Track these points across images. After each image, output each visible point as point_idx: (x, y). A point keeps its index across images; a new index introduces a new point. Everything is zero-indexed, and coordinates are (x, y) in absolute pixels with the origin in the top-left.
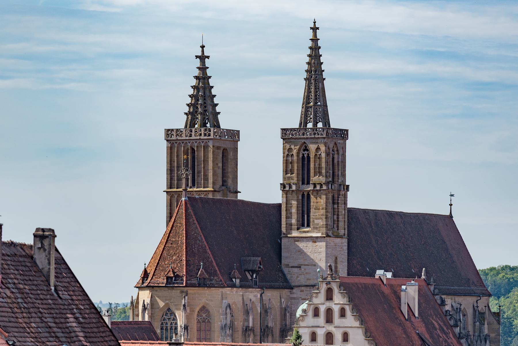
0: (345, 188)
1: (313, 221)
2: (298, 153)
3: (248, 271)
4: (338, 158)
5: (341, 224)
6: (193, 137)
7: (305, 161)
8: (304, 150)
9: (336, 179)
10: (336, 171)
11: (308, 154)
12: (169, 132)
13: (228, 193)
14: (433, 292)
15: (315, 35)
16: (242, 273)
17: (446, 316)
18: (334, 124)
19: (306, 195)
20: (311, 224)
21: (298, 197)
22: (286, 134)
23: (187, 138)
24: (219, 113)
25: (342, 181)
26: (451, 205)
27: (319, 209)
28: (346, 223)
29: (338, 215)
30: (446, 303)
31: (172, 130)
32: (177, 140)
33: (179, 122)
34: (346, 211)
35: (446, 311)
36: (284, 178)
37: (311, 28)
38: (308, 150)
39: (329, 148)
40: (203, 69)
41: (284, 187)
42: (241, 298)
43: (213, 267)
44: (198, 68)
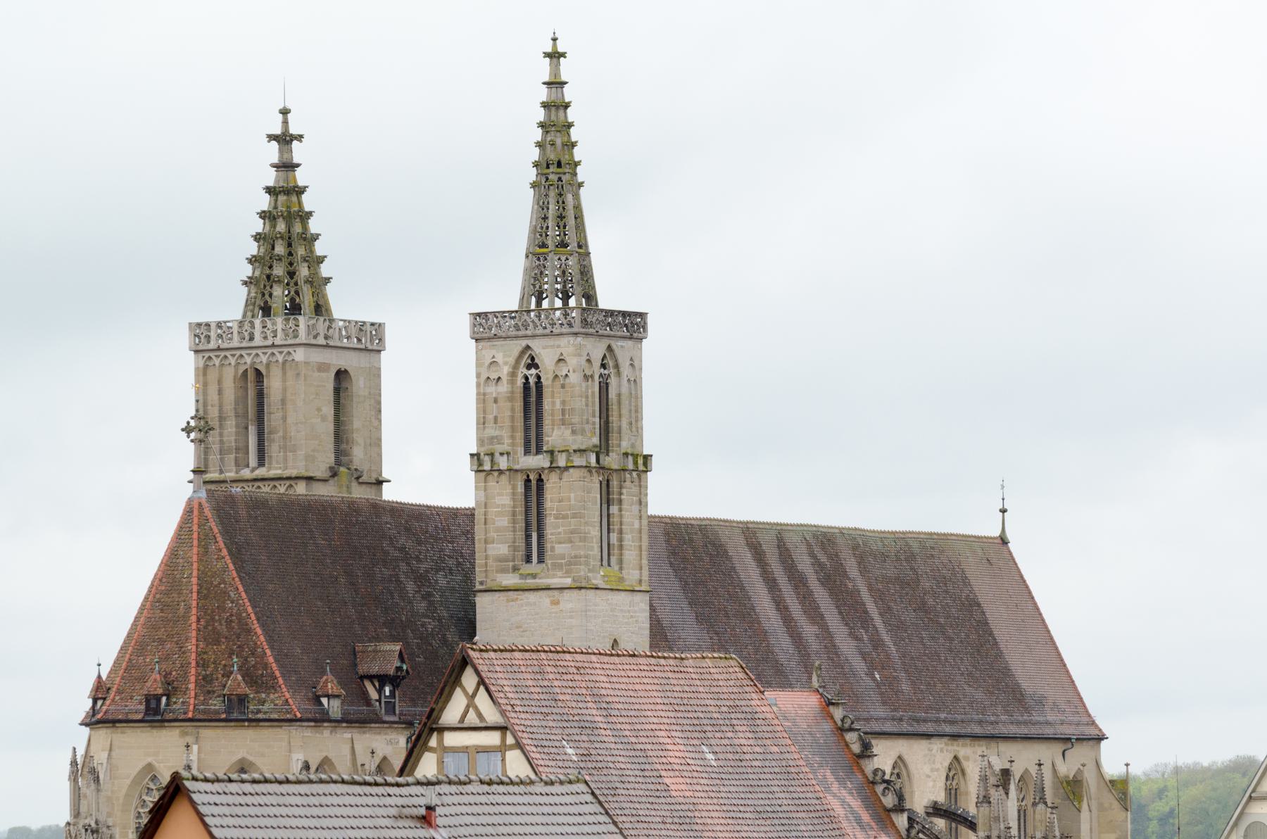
0: (640, 461)
1: (553, 549)
2: (513, 374)
3: (371, 678)
4: (620, 386)
5: (630, 555)
6: (258, 341)
7: (532, 396)
8: (529, 367)
9: (613, 441)
10: (614, 418)
11: (539, 377)
12: (200, 331)
13: (354, 484)
14: (839, 723)
15: (555, 70)
16: (355, 682)
17: (873, 783)
18: (606, 301)
19: (534, 483)
20: (548, 553)
21: (514, 487)
22: (485, 327)
23: (244, 344)
24: (328, 280)
25: (633, 446)
26: (1003, 511)
27: (565, 517)
28: (645, 553)
29: (621, 532)
30: (875, 750)
31: (208, 325)
32: (219, 349)
33: (230, 304)
34: (645, 522)
35: (876, 771)
36: (481, 442)
37: (547, 55)
38: (537, 367)
39: (589, 361)
40: (286, 166)
41: (480, 463)
42: (346, 750)
43: (266, 666)
44: (273, 166)
